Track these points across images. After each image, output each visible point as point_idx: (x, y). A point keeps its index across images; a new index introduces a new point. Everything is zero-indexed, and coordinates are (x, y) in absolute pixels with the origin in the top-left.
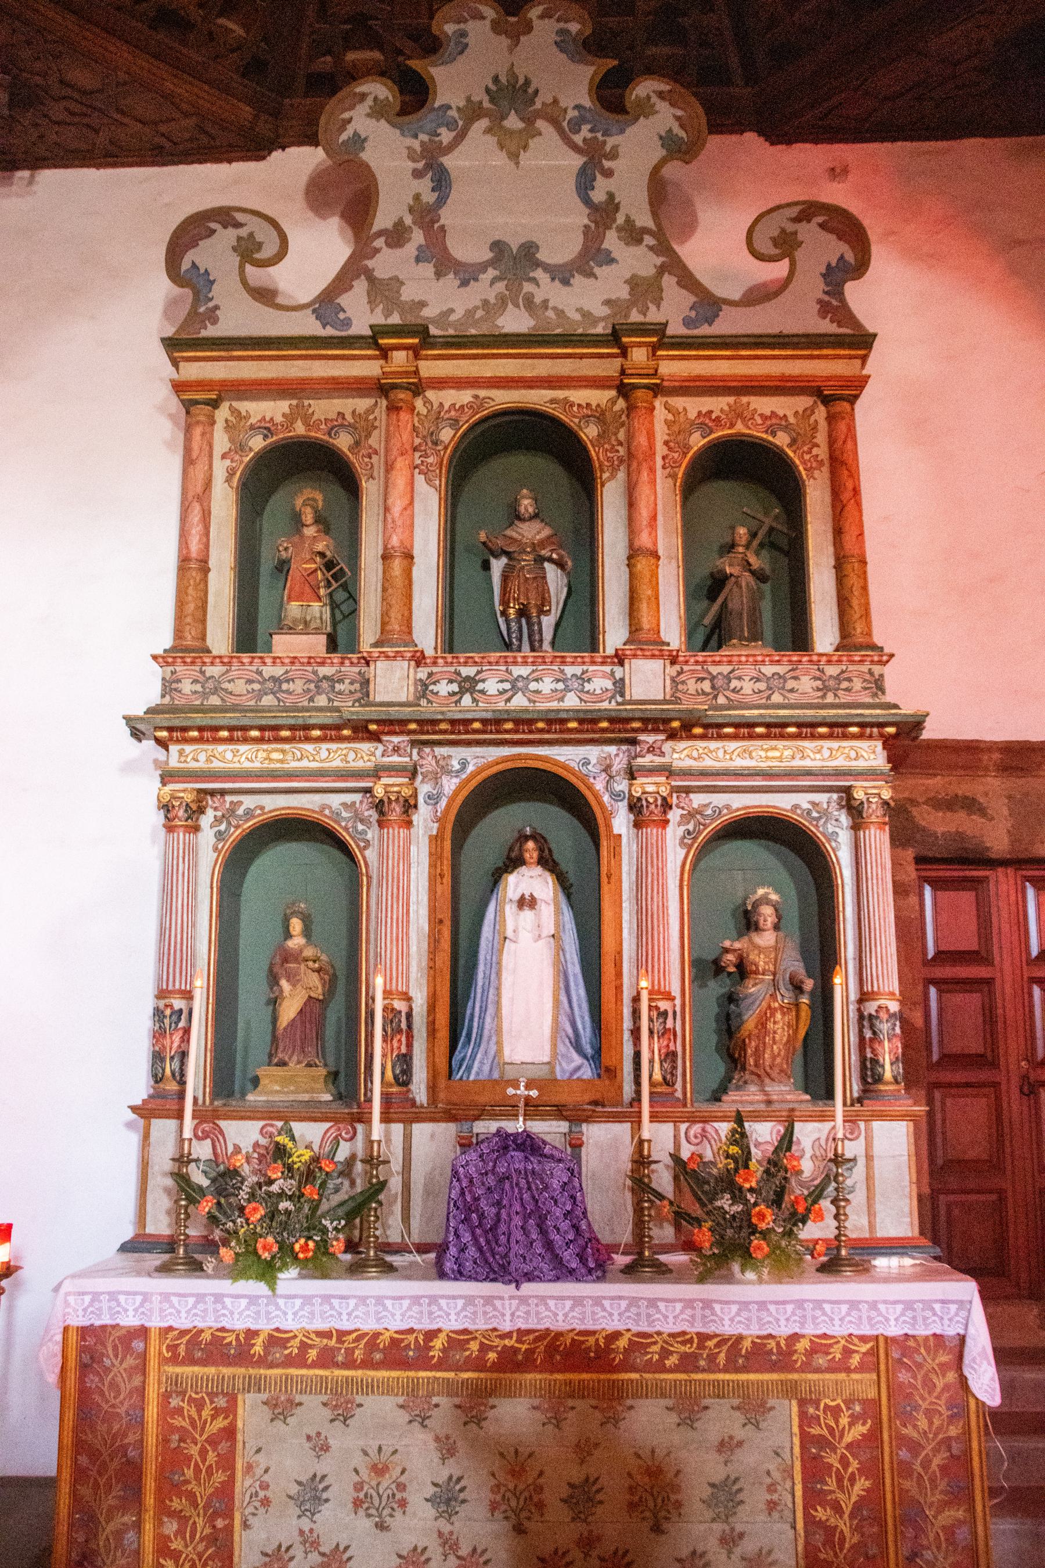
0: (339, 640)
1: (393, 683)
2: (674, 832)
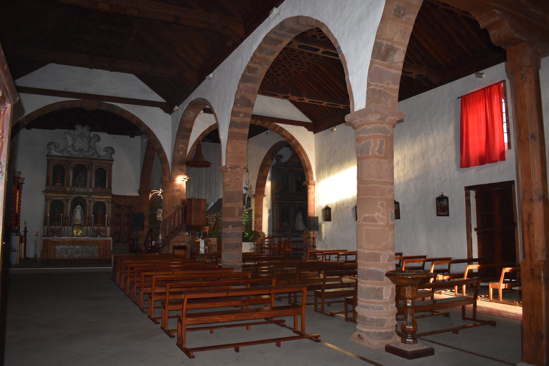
0: (63, 184)
1: (68, 189)
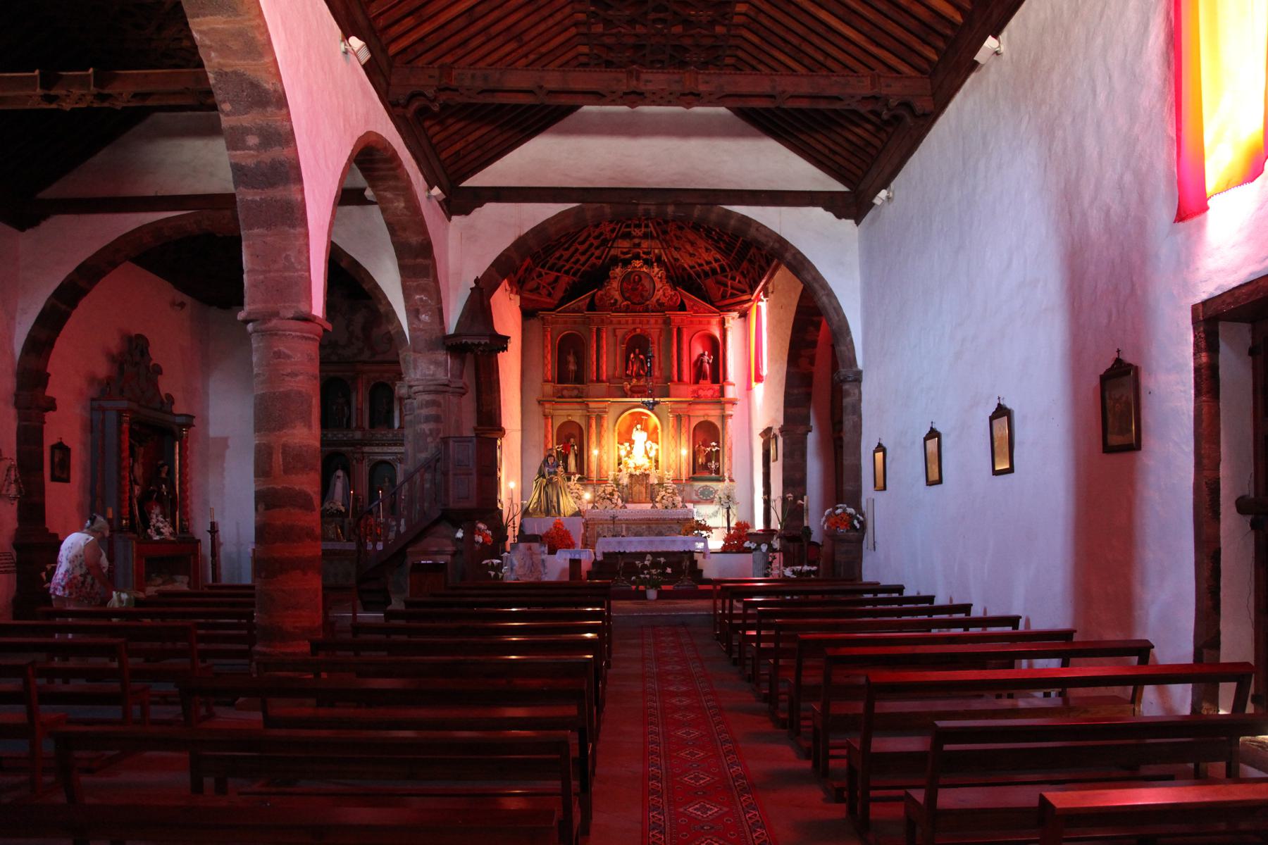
2: (366, 462)
